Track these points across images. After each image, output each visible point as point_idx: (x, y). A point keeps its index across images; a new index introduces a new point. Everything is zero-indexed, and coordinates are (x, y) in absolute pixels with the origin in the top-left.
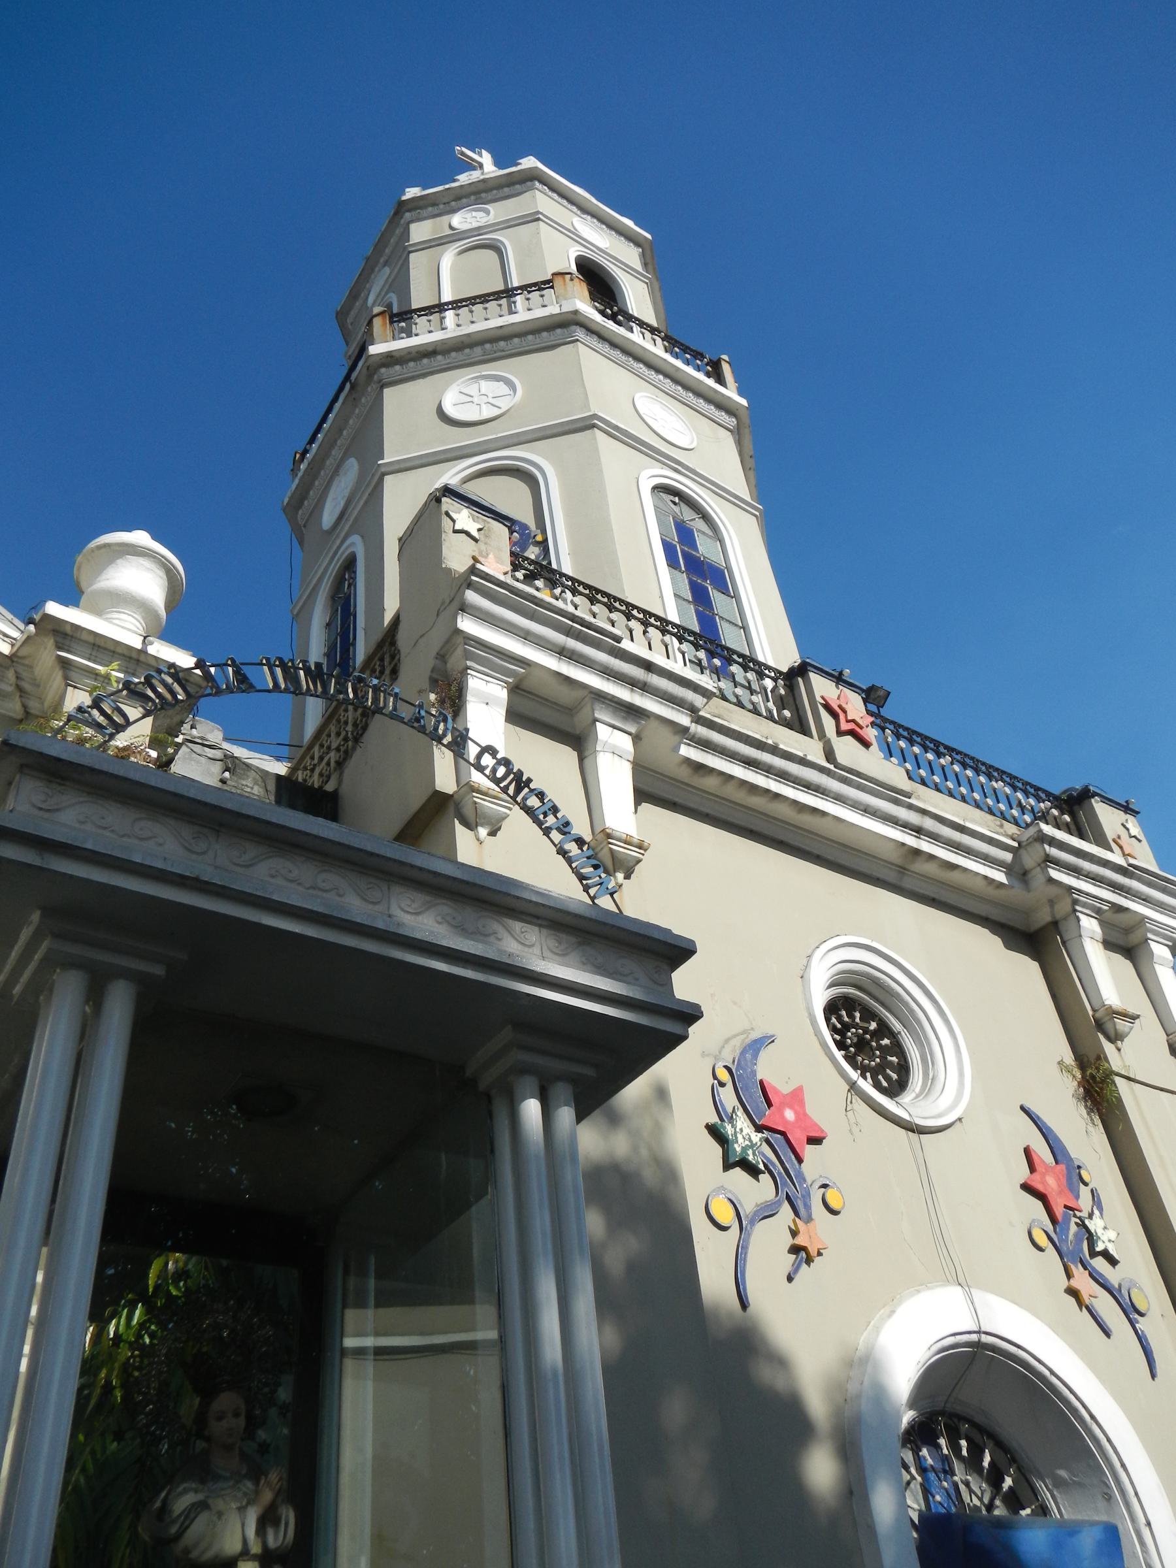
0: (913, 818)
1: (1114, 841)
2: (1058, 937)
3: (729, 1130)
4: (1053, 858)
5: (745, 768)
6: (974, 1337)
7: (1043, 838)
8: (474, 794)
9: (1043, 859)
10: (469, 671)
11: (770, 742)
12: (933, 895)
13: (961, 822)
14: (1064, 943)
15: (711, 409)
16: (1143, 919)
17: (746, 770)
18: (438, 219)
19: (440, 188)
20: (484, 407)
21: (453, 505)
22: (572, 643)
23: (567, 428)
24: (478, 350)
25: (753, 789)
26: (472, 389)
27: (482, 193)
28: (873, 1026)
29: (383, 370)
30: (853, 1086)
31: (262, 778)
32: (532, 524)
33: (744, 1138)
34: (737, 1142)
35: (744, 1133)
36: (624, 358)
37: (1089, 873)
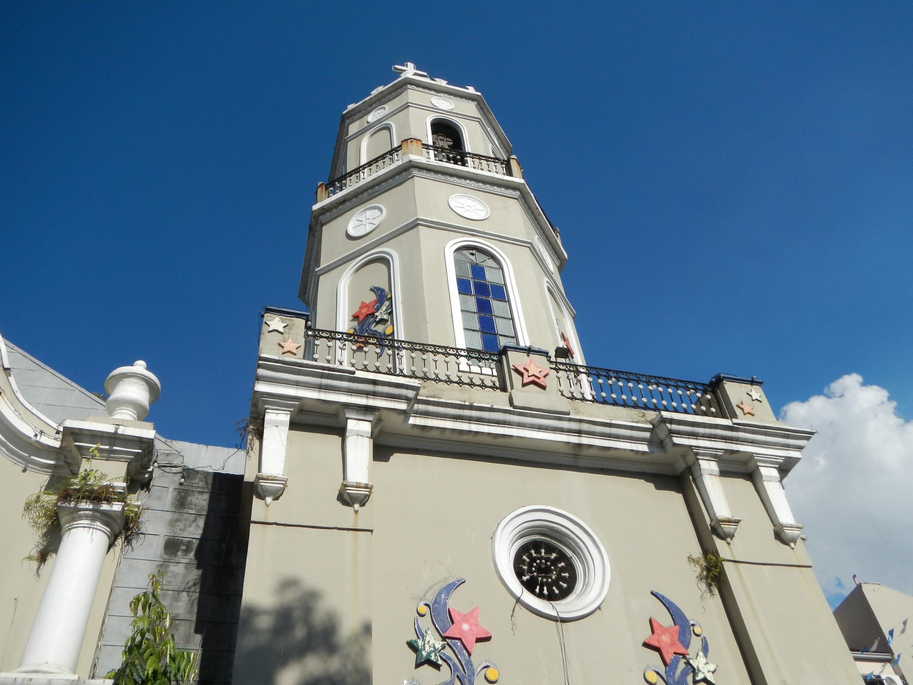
0: (574, 426)
1: (738, 406)
2: (690, 477)
3: (420, 643)
5: (454, 421)
7: (664, 421)
8: (261, 481)
9: (668, 433)
10: (267, 411)
11: (467, 403)
12: (601, 467)
13: (609, 421)
14: (694, 480)
16: (751, 455)
18: (362, 119)
19: (361, 102)
20: (367, 225)
21: (270, 316)
22: (325, 381)
23: (404, 229)
24: (365, 194)
25: (461, 432)
26: (362, 218)
27: (381, 100)
28: (554, 555)
29: (321, 217)
30: (518, 600)
31: (204, 476)
32: (387, 290)
33: (430, 647)
34: (424, 649)
35: (430, 644)
36: (443, 177)
37: (704, 434)
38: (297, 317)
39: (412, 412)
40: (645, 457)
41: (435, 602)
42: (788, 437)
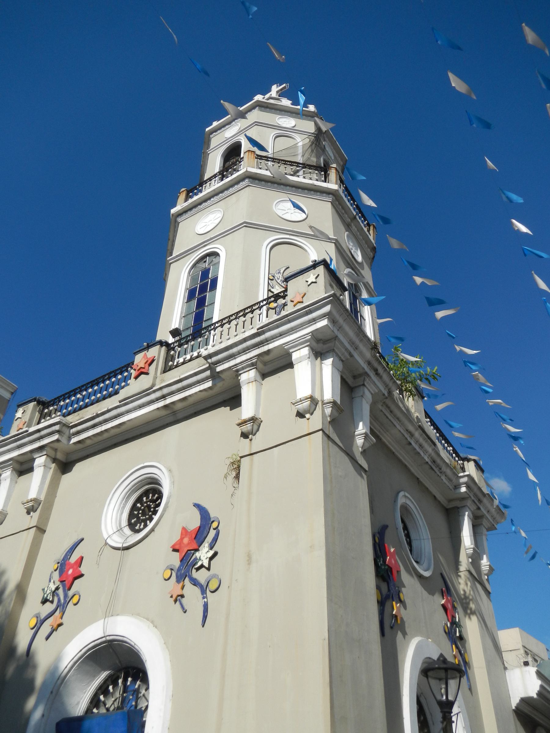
0: (158, 394)
3: (45, 590)
4: (215, 362)
5: (93, 429)
6: (104, 639)
11: (95, 414)
13: (178, 378)
15: (237, 187)
17: (94, 430)
30: (106, 544)
37: (238, 352)
38: (30, 403)
39: (71, 435)
40: (210, 393)
41: (63, 559)
42: (311, 312)
